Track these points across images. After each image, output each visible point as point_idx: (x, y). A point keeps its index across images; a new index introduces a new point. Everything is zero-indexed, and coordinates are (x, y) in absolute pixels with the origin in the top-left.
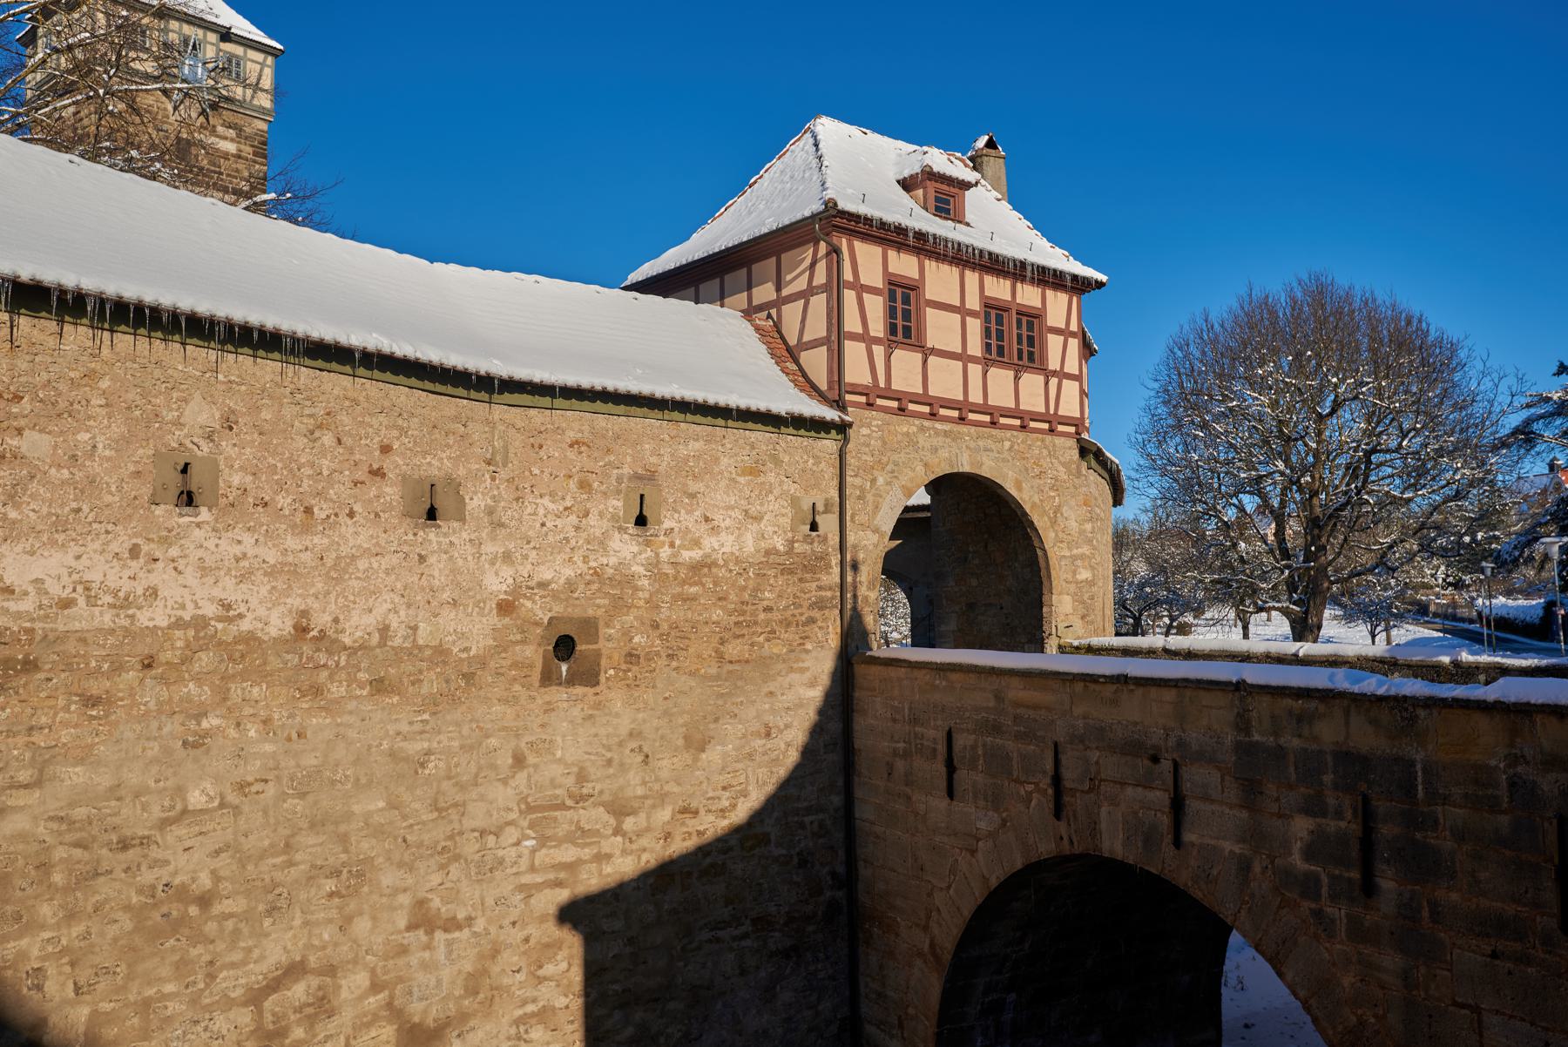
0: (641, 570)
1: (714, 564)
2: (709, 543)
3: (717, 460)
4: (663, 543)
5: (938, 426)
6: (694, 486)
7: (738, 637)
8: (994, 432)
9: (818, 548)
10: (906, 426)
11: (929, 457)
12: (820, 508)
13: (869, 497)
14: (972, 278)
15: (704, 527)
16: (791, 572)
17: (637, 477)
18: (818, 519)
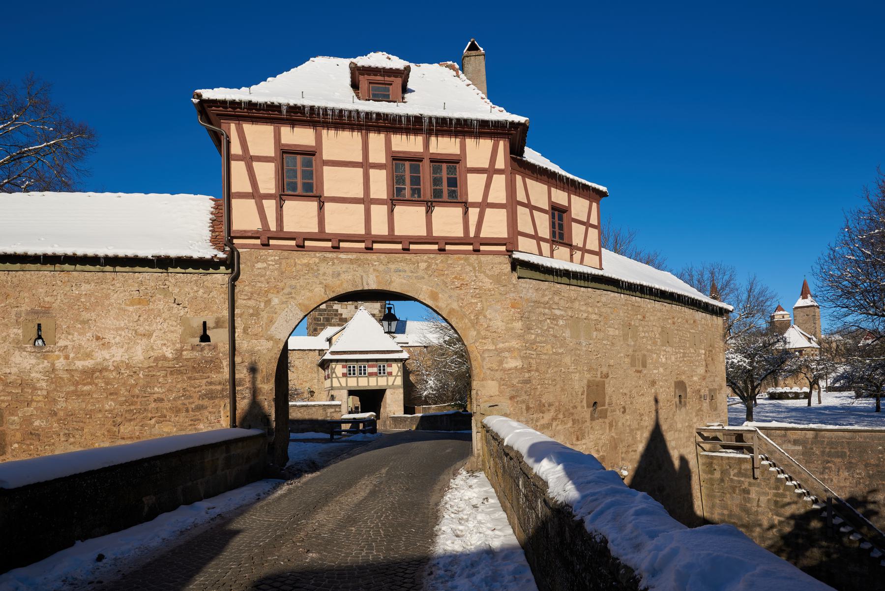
0: (39, 376)
1: (106, 369)
2: (101, 356)
3: (107, 297)
4: (58, 357)
5: (343, 256)
6: (85, 315)
7: (130, 420)
8: (407, 256)
9: (208, 354)
10: (303, 259)
11: (330, 280)
12: (210, 324)
13: (264, 314)
14: (377, 140)
15: (95, 344)
16: (180, 372)
17: (33, 312)
18: (208, 332)
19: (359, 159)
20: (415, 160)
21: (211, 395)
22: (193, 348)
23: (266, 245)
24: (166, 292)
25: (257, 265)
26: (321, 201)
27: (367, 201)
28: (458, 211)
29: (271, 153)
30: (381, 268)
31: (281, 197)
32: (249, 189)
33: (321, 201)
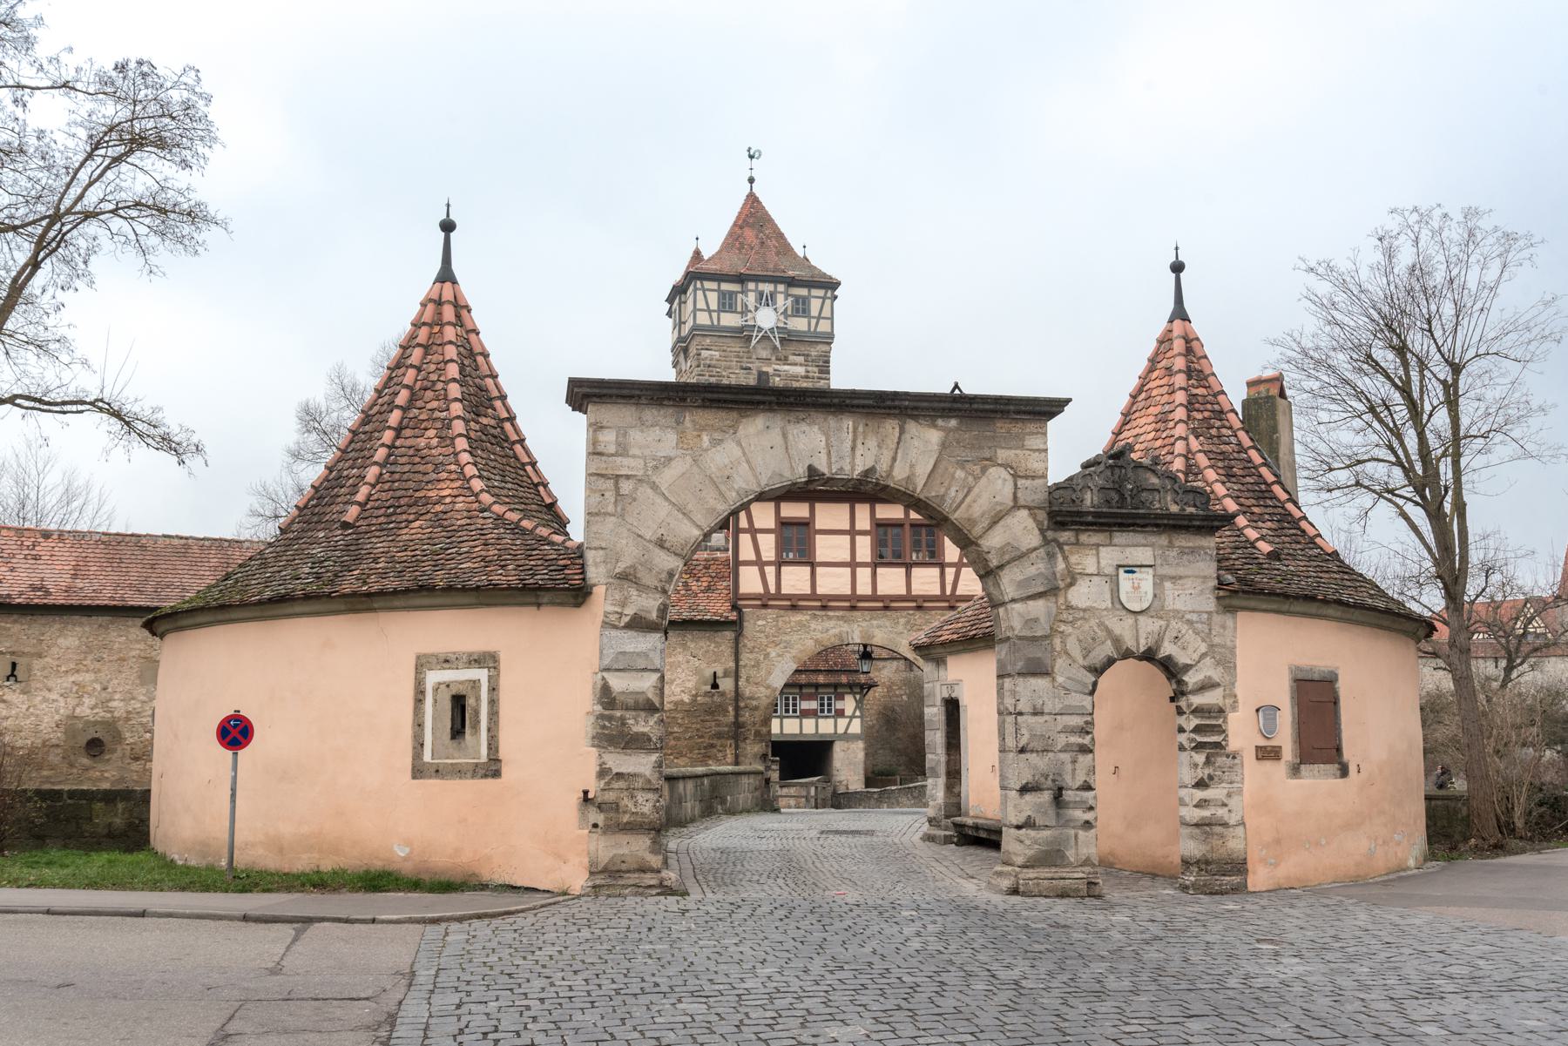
5: (831, 613)
11: (819, 636)
12: (720, 674)
19: (847, 527)
20: (897, 524)
21: (719, 736)
22: (706, 694)
23: (765, 606)
24: (684, 647)
25: (758, 624)
26: (813, 565)
27: (853, 565)
28: (936, 571)
29: (772, 525)
30: (864, 624)
31: (779, 564)
32: (753, 557)
33: (813, 565)
